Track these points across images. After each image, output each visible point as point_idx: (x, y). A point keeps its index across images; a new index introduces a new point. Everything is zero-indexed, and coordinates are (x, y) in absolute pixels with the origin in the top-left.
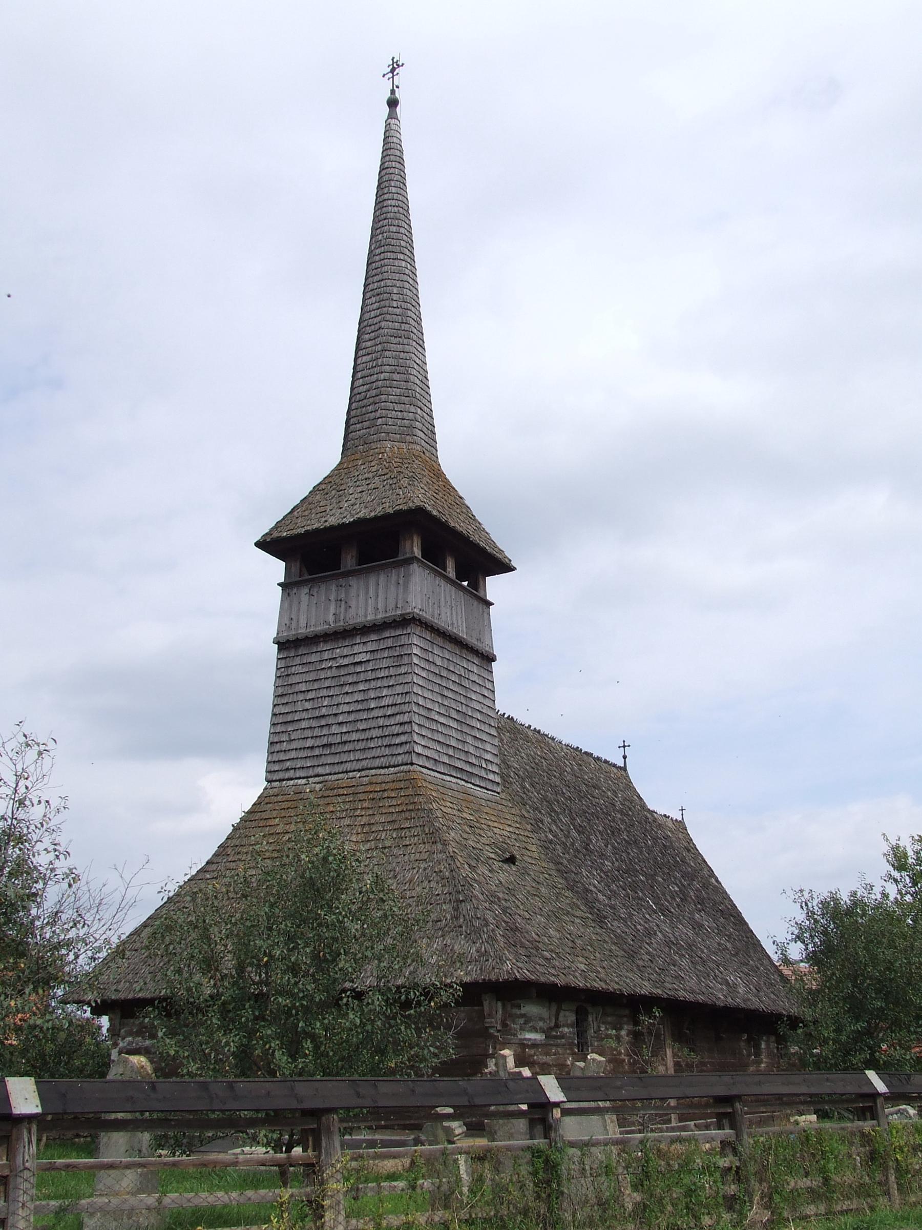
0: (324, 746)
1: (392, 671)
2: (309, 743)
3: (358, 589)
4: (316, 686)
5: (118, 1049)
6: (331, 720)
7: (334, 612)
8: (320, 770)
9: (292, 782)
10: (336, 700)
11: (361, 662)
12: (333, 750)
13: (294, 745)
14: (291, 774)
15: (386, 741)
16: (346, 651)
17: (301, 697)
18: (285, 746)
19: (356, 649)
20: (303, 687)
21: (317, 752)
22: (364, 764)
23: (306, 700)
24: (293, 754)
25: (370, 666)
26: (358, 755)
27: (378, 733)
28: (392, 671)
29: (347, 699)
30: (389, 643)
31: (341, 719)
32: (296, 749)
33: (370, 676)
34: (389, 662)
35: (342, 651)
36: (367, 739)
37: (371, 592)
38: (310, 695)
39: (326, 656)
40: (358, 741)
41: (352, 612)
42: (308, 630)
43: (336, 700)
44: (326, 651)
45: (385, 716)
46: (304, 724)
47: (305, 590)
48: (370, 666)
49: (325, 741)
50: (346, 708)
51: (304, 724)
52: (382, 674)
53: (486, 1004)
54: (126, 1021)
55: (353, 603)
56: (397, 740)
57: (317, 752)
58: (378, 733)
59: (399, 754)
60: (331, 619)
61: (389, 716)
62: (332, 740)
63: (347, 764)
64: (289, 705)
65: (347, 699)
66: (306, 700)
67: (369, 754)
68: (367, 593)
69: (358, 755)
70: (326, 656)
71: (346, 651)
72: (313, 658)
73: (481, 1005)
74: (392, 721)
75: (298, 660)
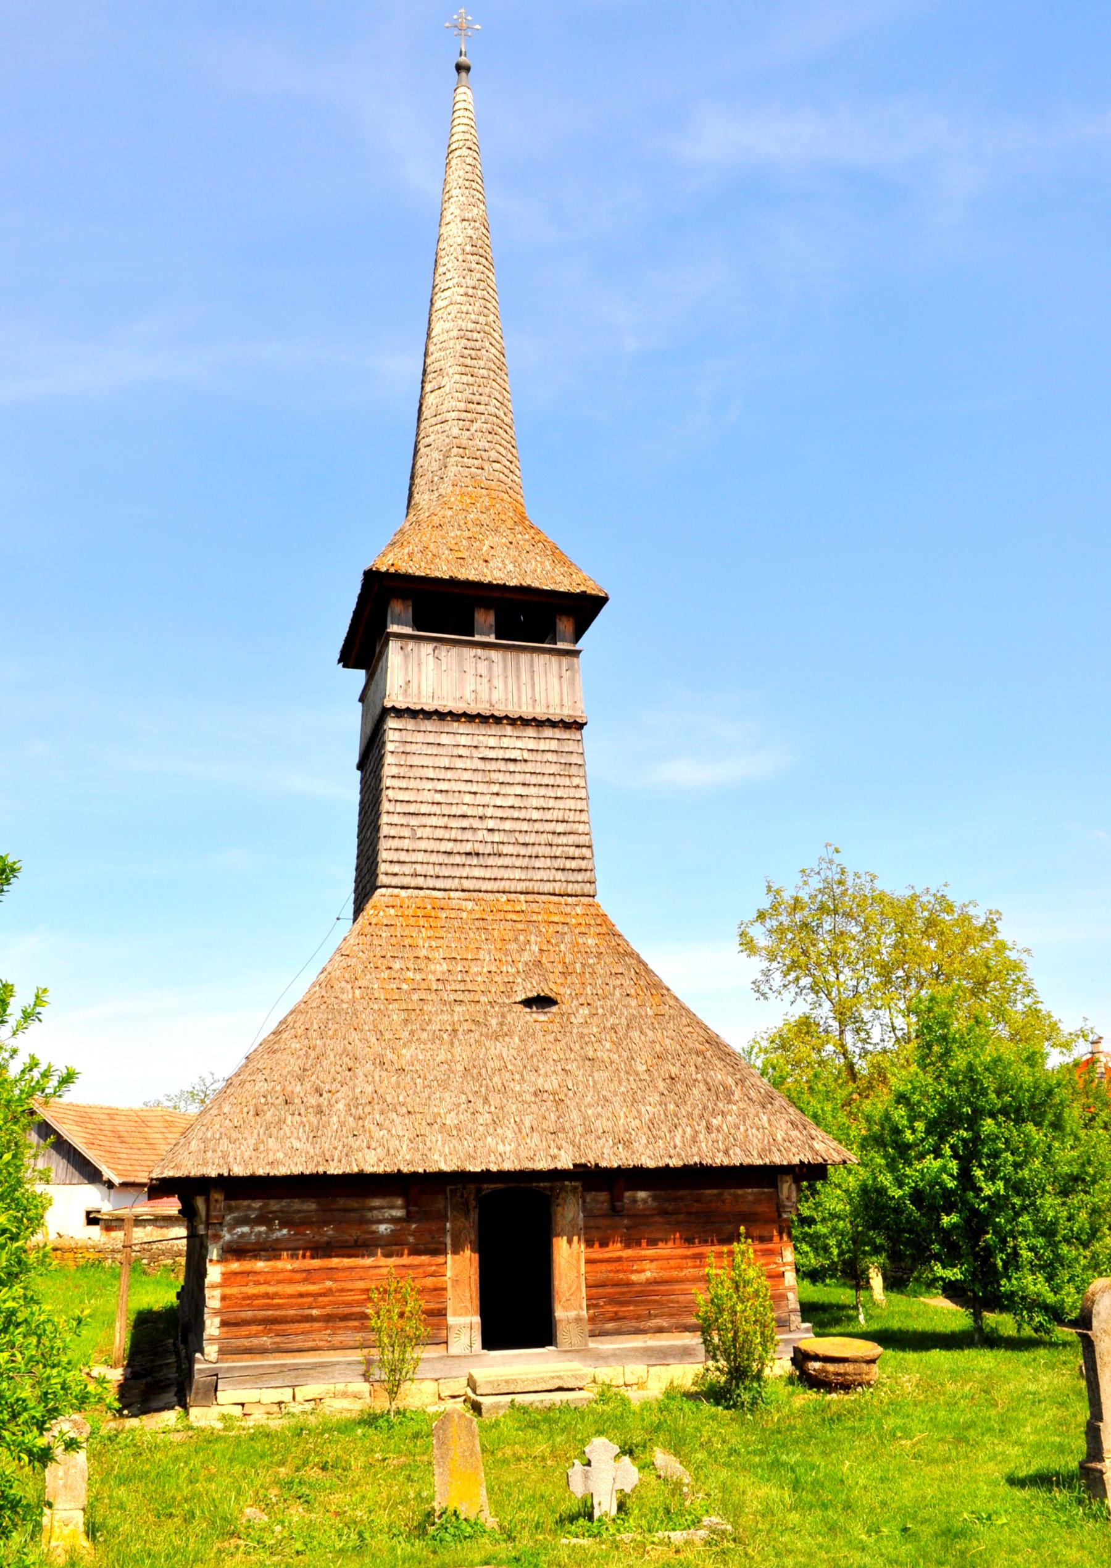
0: (468, 854)
1: (559, 781)
2: (448, 846)
3: (505, 668)
4: (449, 775)
5: (221, 1242)
6: (476, 823)
7: (473, 688)
8: (467, 884)
9: (422, 893)
10: (480, 800)
11: (515, 760)
12: (482, 861)
13: (423, 845)
14: (420, 881)
15: (559, 863)
16: (492, 742)
17: (429, 785)
18: (405, 844)
19: (506, 742)
20: (431, 773)
21: (458, 859)
22: (530, 886)
23: (436, 791)
24: (420, 857)
25: (529, 767)
26: (518, 874)
27: (547, 851)
28: (559, 781)
29: (499, 801)
30: (553, 745)
31: (491, 824)
32: (425, 851)
33: (528, 779)
34: (553, 769)
35: (488, 738)
36: (530, 857)
37: (525, 677)
38: (442, 786)
39: (463, 740)
40: (518, 856)
41: (496, 696)
42: (436, 702)
43: (480, 800)
44: (464, 735)
45: (554, 833)
46: (433, 821)
47: (427, 648)
48: (529, 767)
49: (468, 847)
50: (499, 813)
51: (433, 821)
52: (546, 780)
53: (786, 1186)
54: (233, 1203)
55: (498, 682)
56: (573, 864)
57: (458, 859)
58: (547, 851)
59: (577, 882)
60: (469, 696)
61: (559, 834)
62: (480, 848)
63: (503, 882)
64: (407, 792)
65: (499, 801)
66: (436, 791)
67: (530, 874)
68: (518, 677)
69: (518, 874)
70: (463, 740)
71: (492, 742)
72: (444, 739)
73: (776, 1187)
74: (563, 840)
75: (420, 737)
